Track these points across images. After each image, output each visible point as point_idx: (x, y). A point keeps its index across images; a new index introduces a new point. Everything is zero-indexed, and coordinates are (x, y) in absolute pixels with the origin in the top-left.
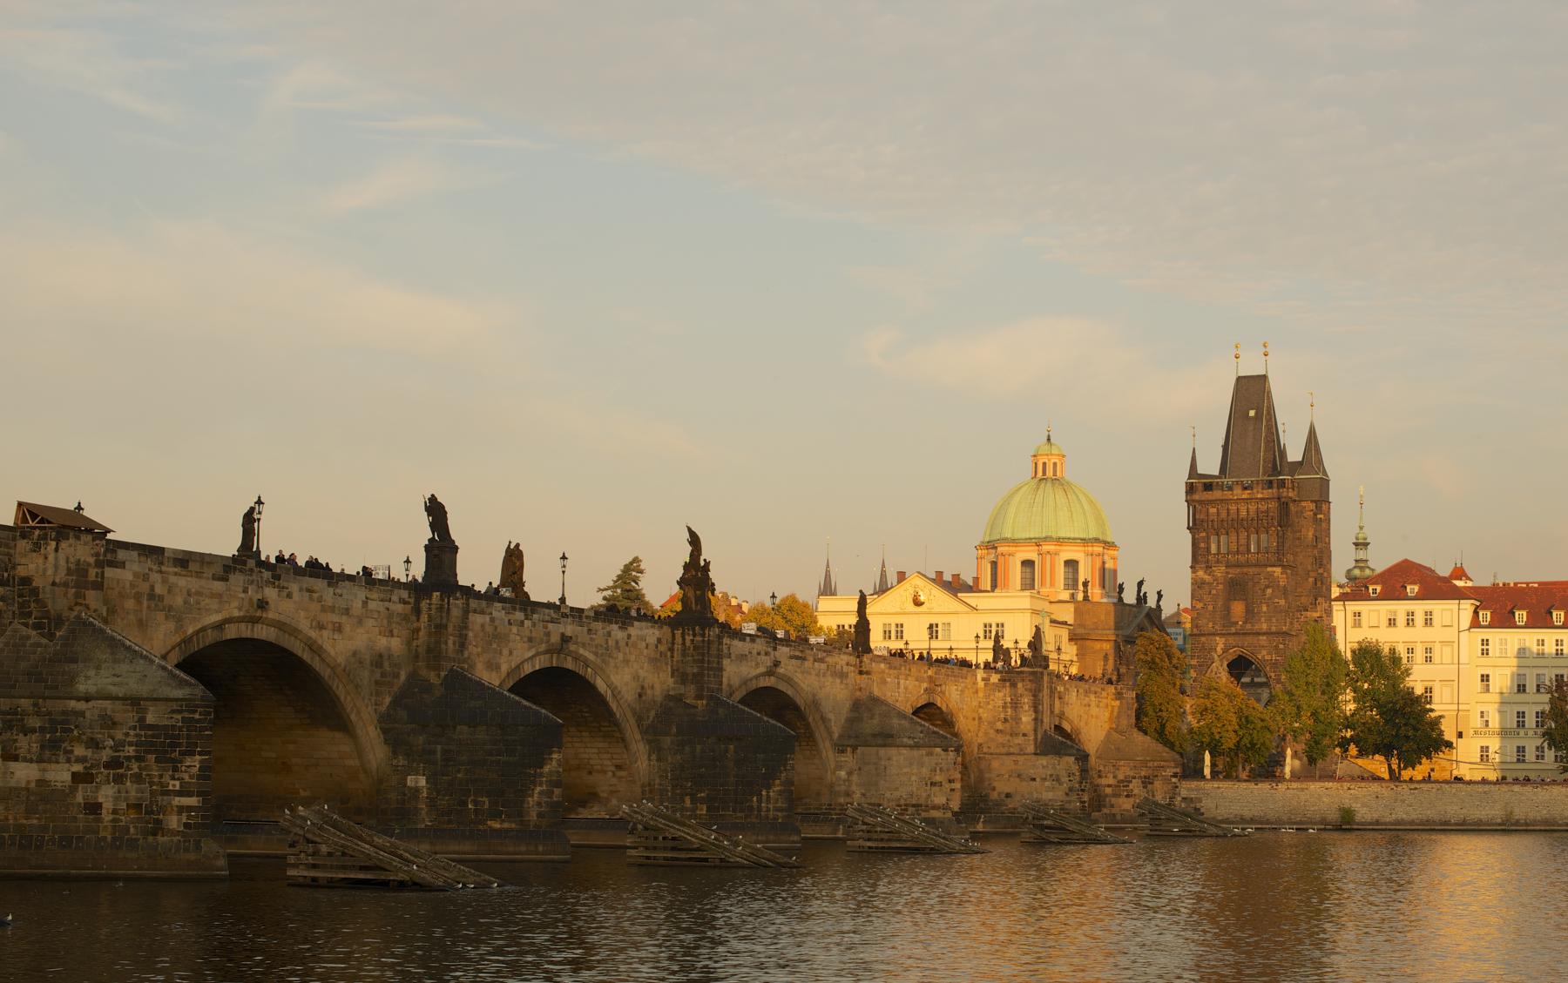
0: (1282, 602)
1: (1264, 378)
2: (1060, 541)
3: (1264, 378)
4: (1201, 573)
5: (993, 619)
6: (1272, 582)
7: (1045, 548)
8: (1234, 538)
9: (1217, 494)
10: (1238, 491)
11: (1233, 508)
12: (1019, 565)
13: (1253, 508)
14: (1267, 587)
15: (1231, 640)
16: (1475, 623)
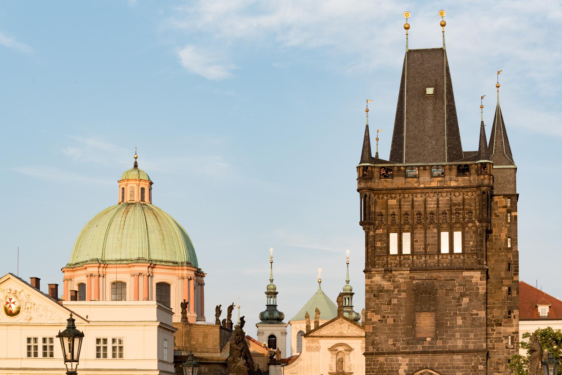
0: (482, 314)
2: (152, 264)
4: (377, 279)
6: (469, 289)
8: (419, 236)
9: (399, 182)
10: (425, 180)
11: (419, 199)
13: (444, 199)
14: (463, 295)
15: (417, 359)
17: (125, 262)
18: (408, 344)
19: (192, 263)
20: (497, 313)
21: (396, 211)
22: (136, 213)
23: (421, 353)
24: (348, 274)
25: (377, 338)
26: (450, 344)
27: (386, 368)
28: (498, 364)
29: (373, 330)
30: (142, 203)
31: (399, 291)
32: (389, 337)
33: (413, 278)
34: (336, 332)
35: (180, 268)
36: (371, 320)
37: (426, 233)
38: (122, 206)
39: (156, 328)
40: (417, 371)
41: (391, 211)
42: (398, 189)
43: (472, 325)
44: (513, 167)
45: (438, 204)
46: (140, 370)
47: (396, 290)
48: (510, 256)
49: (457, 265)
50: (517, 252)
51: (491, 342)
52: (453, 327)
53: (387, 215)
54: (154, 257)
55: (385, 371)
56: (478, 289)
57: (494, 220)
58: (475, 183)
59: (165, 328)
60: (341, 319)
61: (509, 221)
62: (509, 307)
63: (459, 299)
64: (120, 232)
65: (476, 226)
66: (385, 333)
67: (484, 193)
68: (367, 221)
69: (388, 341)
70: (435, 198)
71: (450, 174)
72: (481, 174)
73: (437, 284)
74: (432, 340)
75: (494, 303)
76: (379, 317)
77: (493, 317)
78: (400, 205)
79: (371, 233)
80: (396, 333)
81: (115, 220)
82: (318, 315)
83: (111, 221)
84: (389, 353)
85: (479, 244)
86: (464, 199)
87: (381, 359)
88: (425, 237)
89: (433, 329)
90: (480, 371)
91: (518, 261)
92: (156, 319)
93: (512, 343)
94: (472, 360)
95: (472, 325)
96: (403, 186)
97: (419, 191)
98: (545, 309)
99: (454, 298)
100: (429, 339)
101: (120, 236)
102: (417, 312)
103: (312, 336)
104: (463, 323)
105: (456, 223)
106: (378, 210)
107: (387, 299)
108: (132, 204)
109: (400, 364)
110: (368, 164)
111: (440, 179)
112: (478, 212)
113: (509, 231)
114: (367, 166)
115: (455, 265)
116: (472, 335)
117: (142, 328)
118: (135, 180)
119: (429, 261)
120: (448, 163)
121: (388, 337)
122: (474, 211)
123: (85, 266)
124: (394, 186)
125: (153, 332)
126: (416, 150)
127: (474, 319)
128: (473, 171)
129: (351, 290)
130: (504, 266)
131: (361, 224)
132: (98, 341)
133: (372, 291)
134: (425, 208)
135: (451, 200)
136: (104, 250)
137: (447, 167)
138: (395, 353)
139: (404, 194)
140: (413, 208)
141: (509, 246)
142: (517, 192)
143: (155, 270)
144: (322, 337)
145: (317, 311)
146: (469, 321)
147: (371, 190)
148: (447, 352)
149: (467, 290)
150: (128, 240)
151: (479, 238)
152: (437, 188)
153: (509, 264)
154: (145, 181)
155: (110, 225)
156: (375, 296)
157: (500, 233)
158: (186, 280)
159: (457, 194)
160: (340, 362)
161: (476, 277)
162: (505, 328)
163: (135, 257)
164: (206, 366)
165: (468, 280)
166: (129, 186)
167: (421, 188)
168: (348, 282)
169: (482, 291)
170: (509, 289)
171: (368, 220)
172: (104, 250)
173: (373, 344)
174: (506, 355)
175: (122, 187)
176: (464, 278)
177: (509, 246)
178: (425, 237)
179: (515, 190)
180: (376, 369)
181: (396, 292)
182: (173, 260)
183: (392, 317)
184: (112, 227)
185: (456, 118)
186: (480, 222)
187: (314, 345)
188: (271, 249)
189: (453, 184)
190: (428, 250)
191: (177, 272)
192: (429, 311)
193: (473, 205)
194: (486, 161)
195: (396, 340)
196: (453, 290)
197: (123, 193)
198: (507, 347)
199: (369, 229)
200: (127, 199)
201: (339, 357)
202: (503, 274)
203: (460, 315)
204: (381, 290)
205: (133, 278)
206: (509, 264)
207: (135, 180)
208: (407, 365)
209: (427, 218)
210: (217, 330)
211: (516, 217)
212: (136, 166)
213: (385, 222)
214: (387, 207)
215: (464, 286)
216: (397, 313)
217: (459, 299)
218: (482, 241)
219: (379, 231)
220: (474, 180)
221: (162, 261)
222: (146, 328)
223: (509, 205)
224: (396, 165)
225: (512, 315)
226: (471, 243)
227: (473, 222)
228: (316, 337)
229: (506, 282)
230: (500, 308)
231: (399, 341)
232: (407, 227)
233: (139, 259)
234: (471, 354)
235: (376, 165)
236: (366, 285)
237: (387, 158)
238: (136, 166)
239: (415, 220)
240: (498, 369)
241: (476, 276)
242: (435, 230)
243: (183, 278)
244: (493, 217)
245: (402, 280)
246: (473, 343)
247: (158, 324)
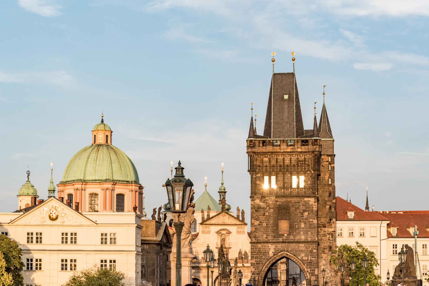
0: (315, 221)
1: (293, 74)
2: (115, 182)
3: (293, 74)
4: (257, 201)
5: (108, 230)
6: (308, 208)
8: (281, 178)
9: (269, 148)
10: (284, 147)
11: (280, 158)
12: (87, 196)
13: (294, 158)
14: (305, 211)
15: (279, 246)
16: (389, 236)
17: (98, 181)
18: (274, 237)
19: (136, 182)
20: (323, 220)
21: (268, 164)
22: (104, 151)
23: (282, 242)
24: (222, 179)
26: (297, 238)
28: (324, 249)
30: (107, 144)
31: (269, 208)
32: (264, 233)
33: (277, 201)
34: (221, 222)
35: (131, 185)
36: (254, 224)
37: (284, 177)
38: (95, 146)
39: (135, 228)
40: (279, 252)
41: (265, 164)
42: (269, 152)
43: (310, 227)
44: (332, 139)
45: (291, 161)
46: (125, 251)
47: (268, 207)
48: (331, 188)
49: (301, 194)
50: (335, 187)
51: (320, 236)
52: (299, 228)
53: (263, 166)
54: (115, 178)
55: (262, 253)
56: (313, 208)
57: (322, 169)
58: (311, 150)
59: (139, 227)
60: (224, 213)
61: (330, 169)
62: (330, 217)
63: (302, 213)
64: (95, 163)
65: (312, 173)
66: (262, 231)
67: (316, 155)
68: (252, 170)
69: (263, 236)
70: (289, 158)
71: (297, 145)
72: (315, 145)
73: (290, 204)
74: (288, 235)
75: (322, 215)
77: (321, 223)
78: (270, 161)
79: (254, 176)
80: (267, 231)
81: (91, 155)
82: (209, 211)
83: (89, 156)
84: (264, 243)
85: (313, 183)
86: (305, 158)
87: (260, 246)
88: (284, 179)
89: (288, 229)
90: (314, 253)
91: (335, 192)
92: (135, 223)
93: (332, 237)
94: (310, 247)
95: (310, 227)
96: (272, 151)
97: (280, 153)
98: (352, 214)
99: (299, 212)
100: (286, 235)
101: (94, 165)
102: (279, 220)
103: (205, 224)
104: (305, 226)
105: (301, 171)
106: (258, 164)
107: (263, 213)
108: (101, 145)
109: (270, 249)
110: (253, 139)
111: (292, 147)
112: (313, 165)
113: (330, 175)
114: (252, 140)
115: (300, 194)
116: (309, 233)
117: (127, 227)
118: (103, 130)
119: (286, 192)
120: (297, 139)
122: (311, 165)
123: (73, 184)
124: (267, 151)
125: (133, 230)
126: (278, 130)
127: (311, 224)
128: (310, 143)
129: (225, 190)
130: (327, 194)
131: (249, 171)
132: (102, 235)
133: (254, 208)
134: (284, 163)
135: (298, 158)
136: (85, 174)
137: (296, 141)
138: (267, 242)
139: (272, 155)
140: (277, 163)
141: (330, 183)
142: (335, 153)
143: (116, 186)
144: (212, 224)
145: (209, 209)
146: (308, 225)
147: (254, 153)
148: (296, 242)
149: (307, 208)
150: (99, 168)
151: (313, 180)
152: (291, 152)
153: (330, 193)
154: (108, 131)
155: (88, 158)
156: (256, 211)
157: (325, 176)
158: (134, 192)
159: (301, 155)
160: (223, 240)
161: (312, 201)
162: (328, 229)
163: (104, 178)
164: (147, 245)
165: (307, 203)
166: (99, 134)
167: (281, 152)
168: (222, 184)
169: (315, 209)
170: (330, 207)
171: (252, 169)
172: (85, 174)
173: (255, 237)
174: (328, 244)
175: (94, 134)
176: (305, 201)
177: (330, 183)
178: (284, 179)
179: (333, 152)
181: (268, 209)
182: (126, 180)
183: (265, 222)
184: (90, 160)
185: (301, 112)
186: (314, 171)
187: (207, 230)
188: (172, 162)
189: (299, 150)
190: (285, 186)
191: (129, 187)
192: (286, 219)
193: (310, 161)
194: (317, 138)
195: (267, 235)
196: (299, 208)
197: (95, 138)
198: (329, 240)
199: (253, 174)
200: (98, 142)
201: (223, 237)
202: (327, 199)
203: (303, 222)
204: (259, 207)
205: (103, 191)
206: (330, 193)
207: (103, 130)
209: (285, 168)
210: (154, 223)
211: (334, 167)
212: (102, 121)
213: (261, 170)
214: (262, 161)
215: (305, 206)
216: (268, 220)
217: (302, 213)
218: (315, 181)
219: (259, 175)
220: (311, 148)
221: (120, 181)
222: (129, 227)
223: (330, 160)
224: (268, 139)
225: (332, 221)
226: (309, 182)
227: (310, 171)
228: (208, 224)
229: (328, 203)
230: (325, 217)
231: (269, 236)
232: (274, 173)
233: (106, 180)
234: (309, 244)
235: (257, 139)
236: (251, 205)
237: (262, 135)
238: (102, 121)
239: (278, 170)
240: (324, 252)
241: (312, 200)
242: (289, 175)
243: (132, 191)
244: (321, 167)
245: (271, 202)
246: (310, 237)
247: (136, 225)
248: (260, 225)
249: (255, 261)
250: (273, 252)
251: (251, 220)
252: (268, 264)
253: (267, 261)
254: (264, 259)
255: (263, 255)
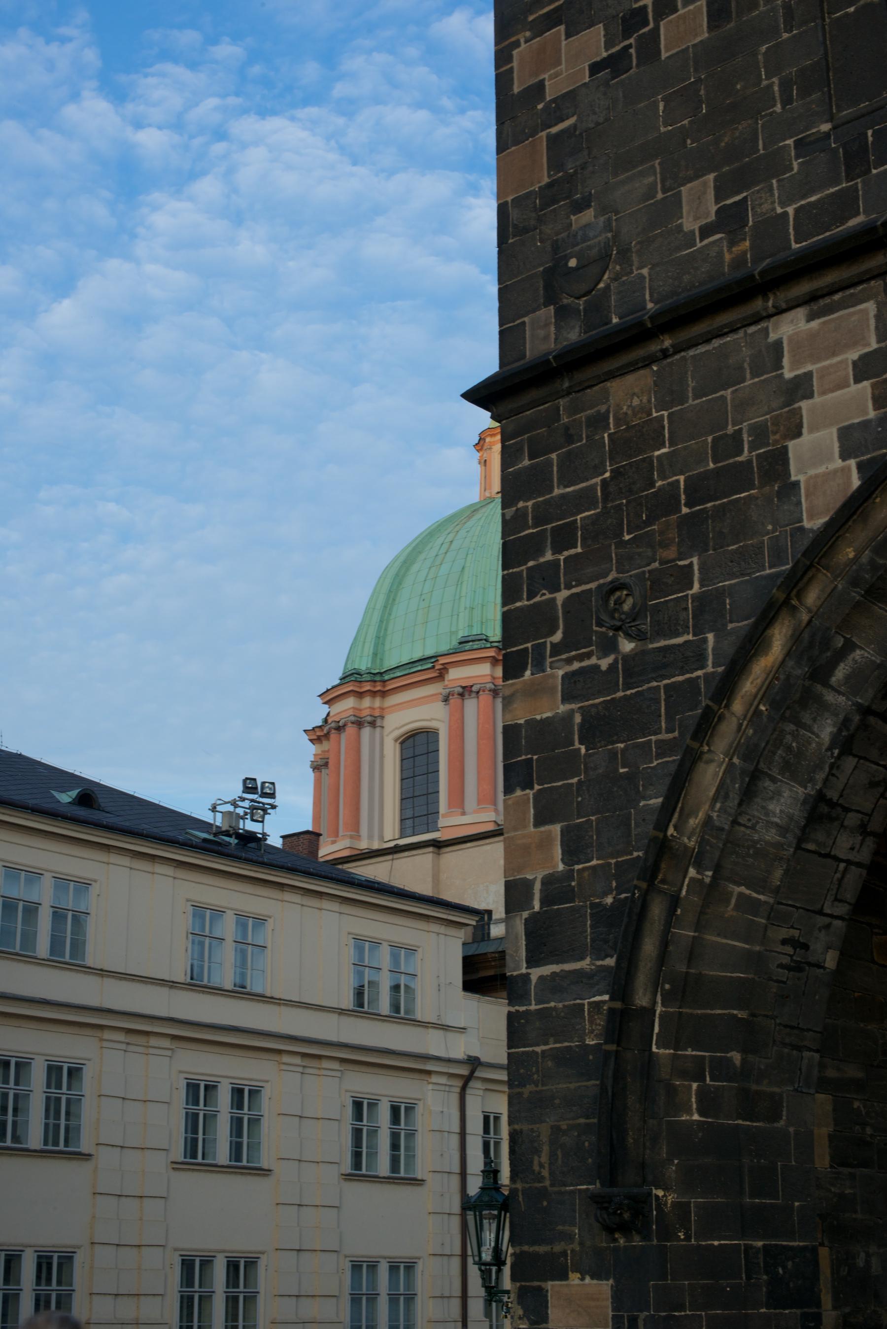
7: (457, 675)
25: (588, 215)
27: (670, 464)
29: (555, 164)
55: (667, 502)
76: (594, 42)
87: (628, 393)
121: (674, 179)
136: (380, 640)
172: (380, 640)
180: (584, 499)
195: (741, 173)
208: (863, 369)
231: (775, 164)
248: (614, 64)
249: (573, 688)
250: (850, 441)
251: (502, 57)
252: (791, 699)
253: (753, 644)
254: (708, 609)
255: (694, 534)
